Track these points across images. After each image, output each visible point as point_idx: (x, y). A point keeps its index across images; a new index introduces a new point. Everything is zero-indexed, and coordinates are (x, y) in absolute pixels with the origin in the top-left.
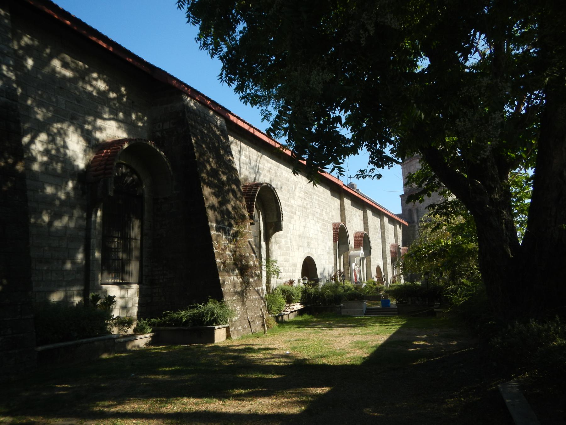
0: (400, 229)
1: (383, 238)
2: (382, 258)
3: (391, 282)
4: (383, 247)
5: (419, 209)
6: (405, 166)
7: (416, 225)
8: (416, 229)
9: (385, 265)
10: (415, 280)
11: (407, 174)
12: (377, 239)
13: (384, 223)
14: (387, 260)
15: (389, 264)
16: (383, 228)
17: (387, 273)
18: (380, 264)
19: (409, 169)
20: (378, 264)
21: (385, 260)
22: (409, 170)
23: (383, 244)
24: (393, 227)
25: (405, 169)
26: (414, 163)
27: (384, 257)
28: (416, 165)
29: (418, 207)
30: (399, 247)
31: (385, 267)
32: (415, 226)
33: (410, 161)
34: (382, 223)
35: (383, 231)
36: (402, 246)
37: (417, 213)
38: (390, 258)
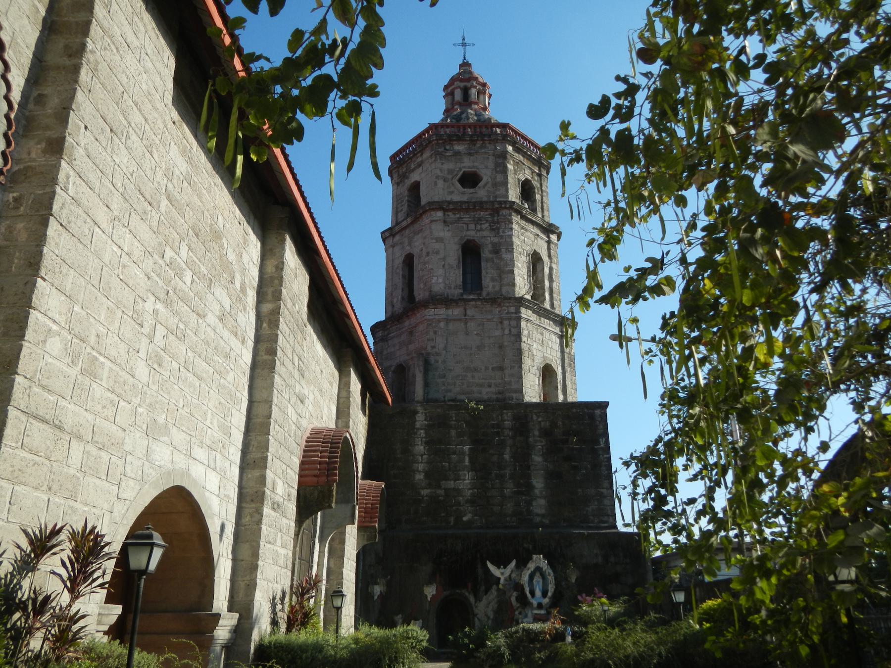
0: (364, 413)
1: (263, 347)
2: (237, 457)
3: (274, 623)
4: (257, 396)
5: (432, 359)
6: (397, 238)
7: (419, 409)
8: (418, 425)
9: (249, 508)
10: (399, 618)
11: (399, 261)
12: (212, 319)
13: (280, 267)
14: (269, 474)
15: (276, 506)
16: (270, 291)
17: (256, 555)
18: (212, 482)
19: (410, 244)
20: (186, 473)
21: (256, 473)
22: (408, 248)
23: (259, 383)
24: (336, 374)
25: (397, 249)
26: (427, 221)
27: (254, 455)
28: (433, 226)
29: (428, 354)
30: (347, 447)
31: (246, 520)
32: (416, 412)
33: (412, 223)
34: (270, 269)
35: (267, 307)
36: (363, 478)
37: (426, 372)
38: (294, 477)
